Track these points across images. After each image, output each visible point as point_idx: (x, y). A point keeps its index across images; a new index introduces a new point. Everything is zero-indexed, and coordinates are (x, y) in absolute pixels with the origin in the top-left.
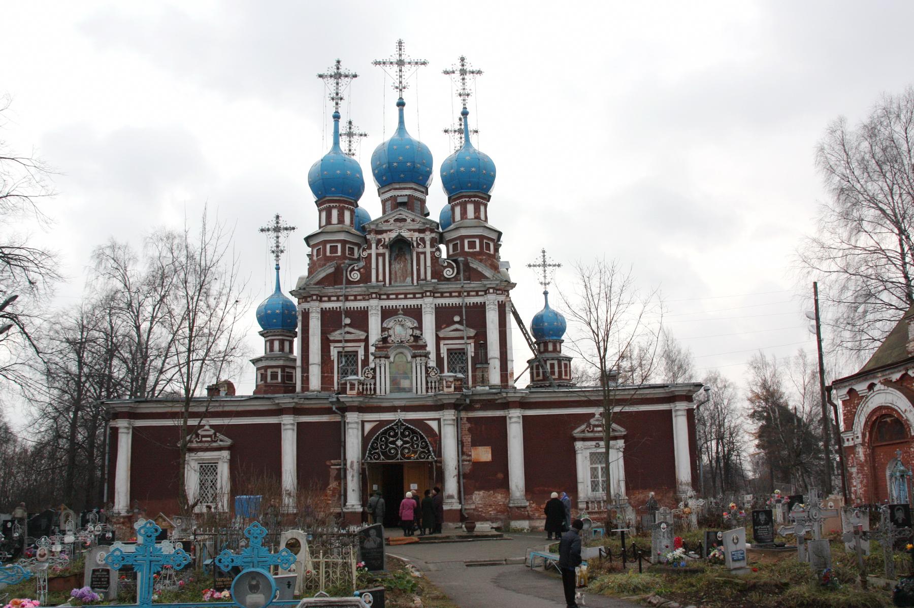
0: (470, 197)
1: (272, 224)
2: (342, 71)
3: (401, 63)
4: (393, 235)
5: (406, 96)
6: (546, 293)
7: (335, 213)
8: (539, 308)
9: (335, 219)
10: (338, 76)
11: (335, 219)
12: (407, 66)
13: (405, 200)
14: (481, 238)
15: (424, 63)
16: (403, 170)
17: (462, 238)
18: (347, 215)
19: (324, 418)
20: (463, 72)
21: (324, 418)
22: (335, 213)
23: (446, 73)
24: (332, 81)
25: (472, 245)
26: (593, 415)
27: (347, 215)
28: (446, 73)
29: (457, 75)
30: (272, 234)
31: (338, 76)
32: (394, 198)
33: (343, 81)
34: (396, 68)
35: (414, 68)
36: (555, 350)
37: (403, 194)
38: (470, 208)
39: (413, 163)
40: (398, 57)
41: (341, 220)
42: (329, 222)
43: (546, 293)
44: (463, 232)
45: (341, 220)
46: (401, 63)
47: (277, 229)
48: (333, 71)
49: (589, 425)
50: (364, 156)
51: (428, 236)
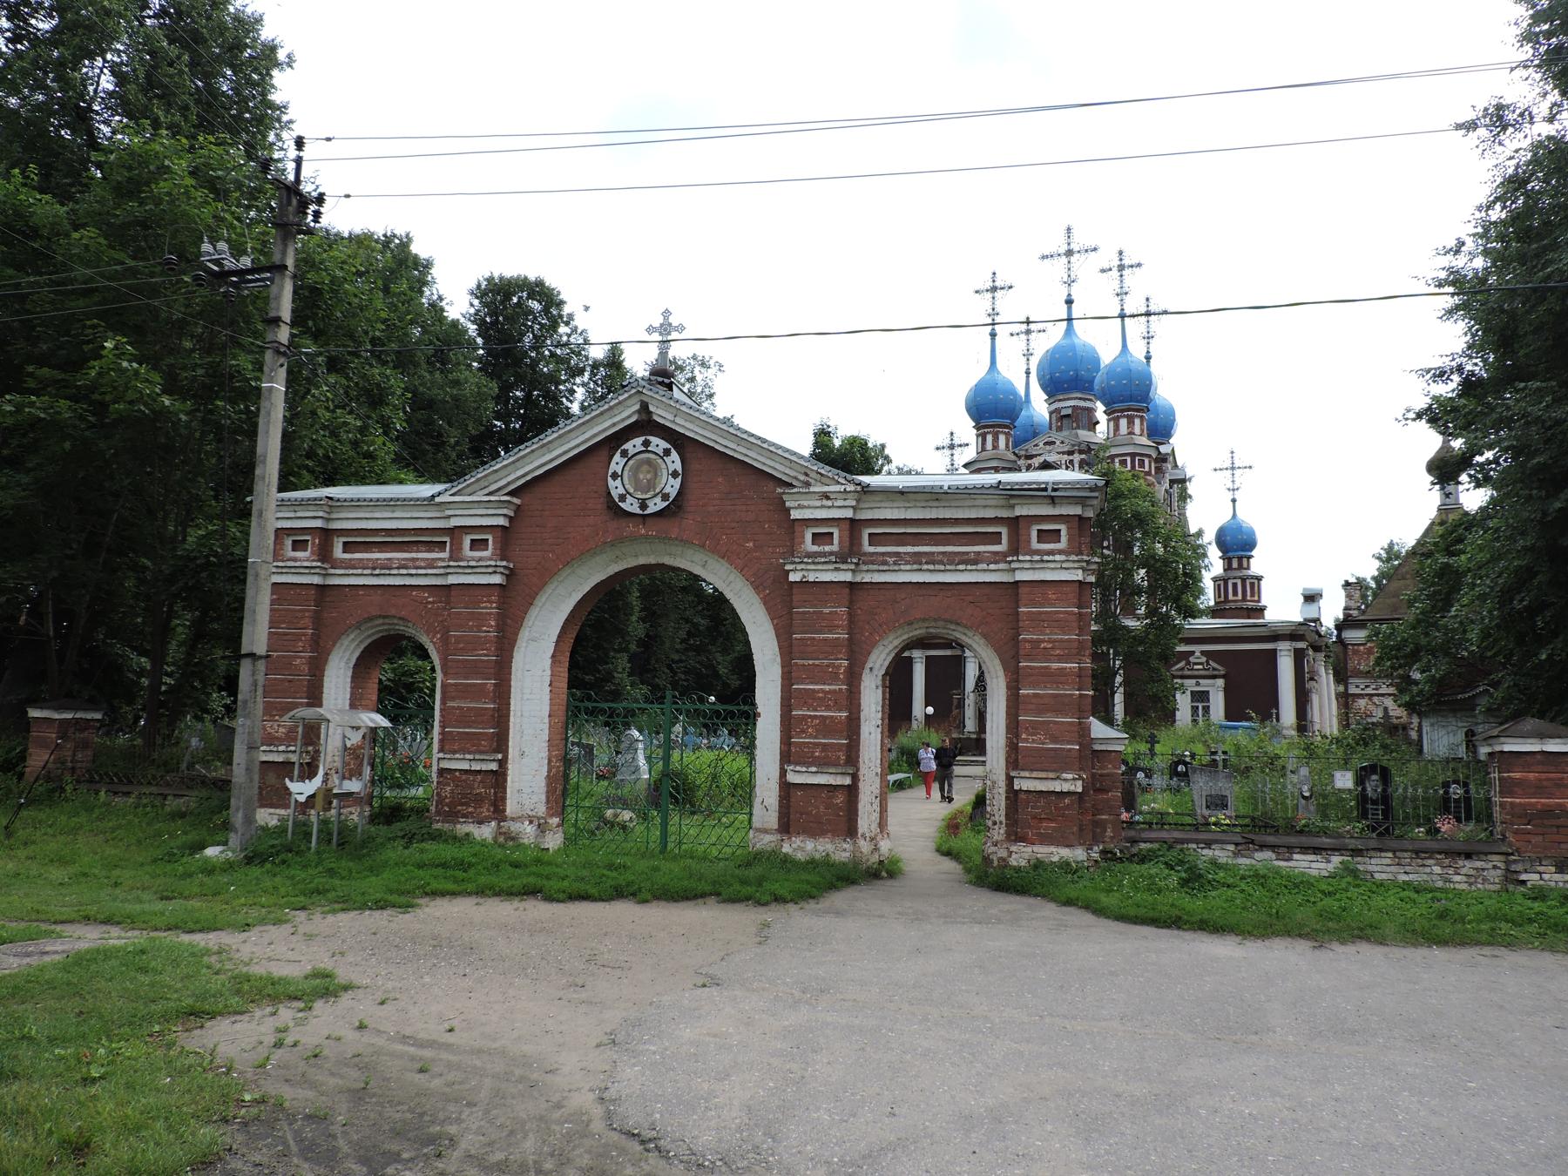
0: (1122, 411)
1: (947, 442)
2: (997, 284)
3: (1069, 253)
4: (1041, 459)
5: (1076, 292)
6: (1234, 501)
7: (989, 438)
8: (1224, 517)
9: (989, 445)
10: (994, 289)
11: (989, 445)
12: (1076, 256)
13: (1069, 411)
14: (1133, 455)
15: (1095, 249)
16: (1068, 377)
17: (1112, 457)
18: (1002, 439)
19: (948, 652)
20: (1121, 268)
21: (948, 652)
22: (989, 438)
23: (1103, 271)
24: (989, 295)
25: (1123, 463)
26: (1193, 653)
27: (1002, 438)
28: (1103, 271)
29: (1115, 273)
30: (947, 452)
31: (994, 289)
32: (1057, 411)
33: (999, 294)
34: (1064, 259)
35: (1083, 256)
36: (1240, 567)
37: (1067, 405)
38: (1123, 422)
39: (1076, 371)
40: (1066, 247)
41: (995, 447)
42: (983, 449)
43: (1234, 501)
44: (1114, 451)
45: (995, 447)
46: (1069, 253)
47: (952, 447)
48: (989, 284)
49: (1188, 663)
50: (1018, 371)
51: (1077, 458)
